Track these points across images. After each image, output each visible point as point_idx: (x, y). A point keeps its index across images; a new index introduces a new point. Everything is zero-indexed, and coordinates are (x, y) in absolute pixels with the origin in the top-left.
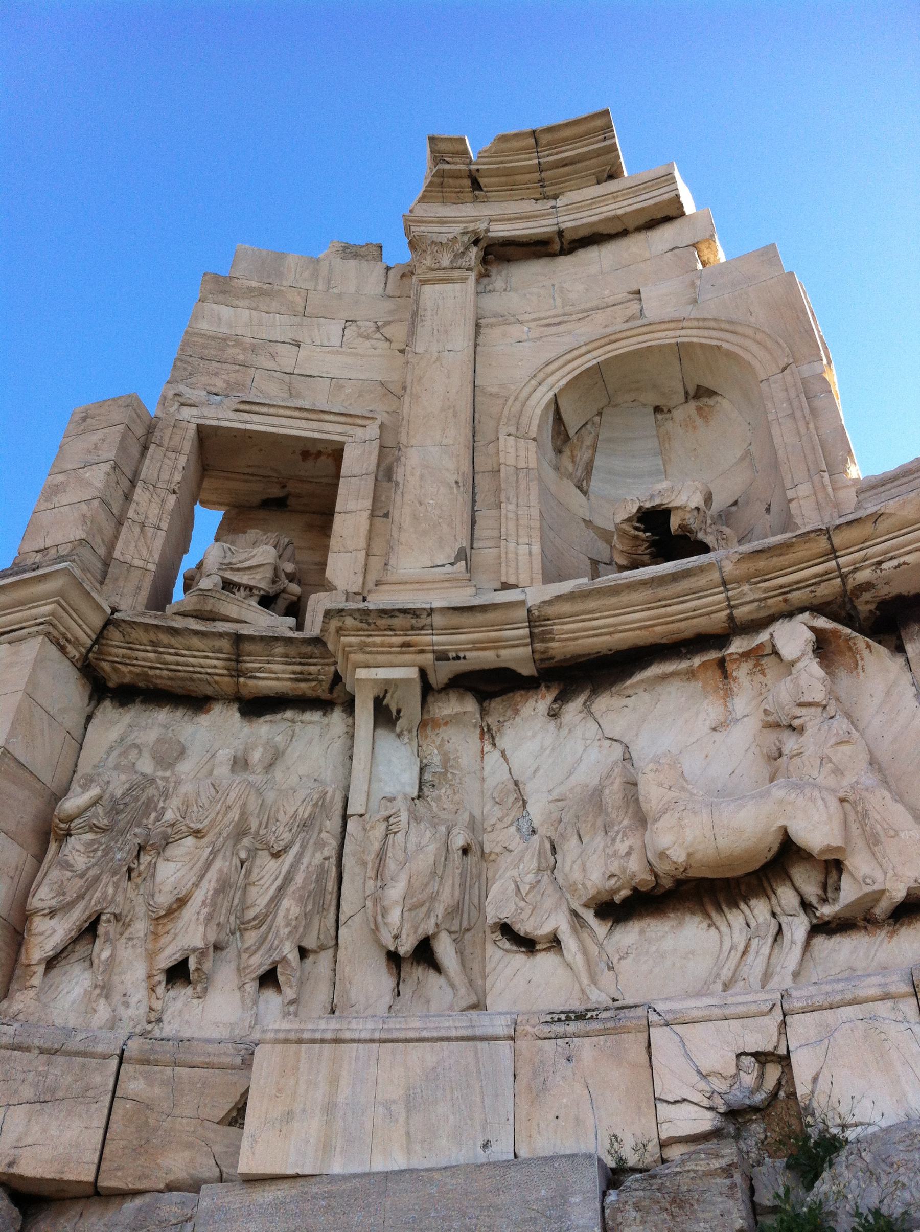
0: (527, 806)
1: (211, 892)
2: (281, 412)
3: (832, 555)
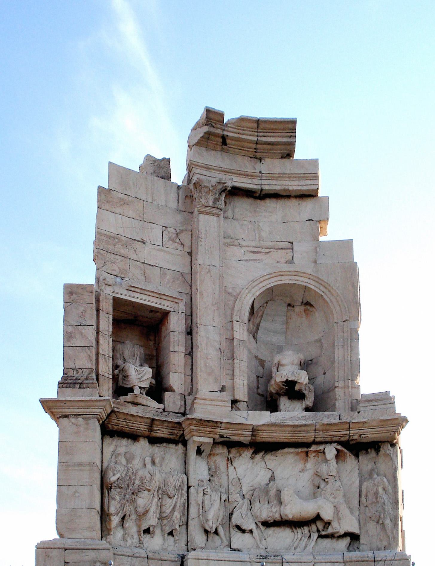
0: (242, 487)
1: (155, 509)
2: (146, 293)
3: (348, 430)
